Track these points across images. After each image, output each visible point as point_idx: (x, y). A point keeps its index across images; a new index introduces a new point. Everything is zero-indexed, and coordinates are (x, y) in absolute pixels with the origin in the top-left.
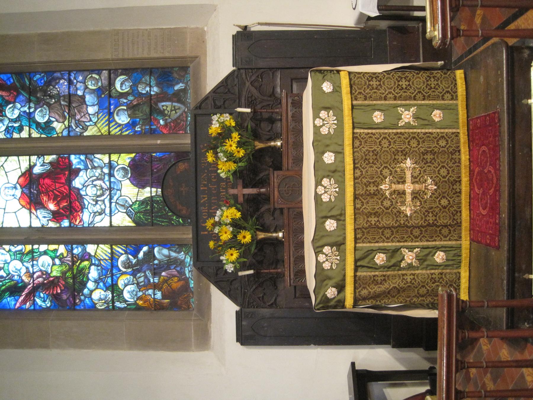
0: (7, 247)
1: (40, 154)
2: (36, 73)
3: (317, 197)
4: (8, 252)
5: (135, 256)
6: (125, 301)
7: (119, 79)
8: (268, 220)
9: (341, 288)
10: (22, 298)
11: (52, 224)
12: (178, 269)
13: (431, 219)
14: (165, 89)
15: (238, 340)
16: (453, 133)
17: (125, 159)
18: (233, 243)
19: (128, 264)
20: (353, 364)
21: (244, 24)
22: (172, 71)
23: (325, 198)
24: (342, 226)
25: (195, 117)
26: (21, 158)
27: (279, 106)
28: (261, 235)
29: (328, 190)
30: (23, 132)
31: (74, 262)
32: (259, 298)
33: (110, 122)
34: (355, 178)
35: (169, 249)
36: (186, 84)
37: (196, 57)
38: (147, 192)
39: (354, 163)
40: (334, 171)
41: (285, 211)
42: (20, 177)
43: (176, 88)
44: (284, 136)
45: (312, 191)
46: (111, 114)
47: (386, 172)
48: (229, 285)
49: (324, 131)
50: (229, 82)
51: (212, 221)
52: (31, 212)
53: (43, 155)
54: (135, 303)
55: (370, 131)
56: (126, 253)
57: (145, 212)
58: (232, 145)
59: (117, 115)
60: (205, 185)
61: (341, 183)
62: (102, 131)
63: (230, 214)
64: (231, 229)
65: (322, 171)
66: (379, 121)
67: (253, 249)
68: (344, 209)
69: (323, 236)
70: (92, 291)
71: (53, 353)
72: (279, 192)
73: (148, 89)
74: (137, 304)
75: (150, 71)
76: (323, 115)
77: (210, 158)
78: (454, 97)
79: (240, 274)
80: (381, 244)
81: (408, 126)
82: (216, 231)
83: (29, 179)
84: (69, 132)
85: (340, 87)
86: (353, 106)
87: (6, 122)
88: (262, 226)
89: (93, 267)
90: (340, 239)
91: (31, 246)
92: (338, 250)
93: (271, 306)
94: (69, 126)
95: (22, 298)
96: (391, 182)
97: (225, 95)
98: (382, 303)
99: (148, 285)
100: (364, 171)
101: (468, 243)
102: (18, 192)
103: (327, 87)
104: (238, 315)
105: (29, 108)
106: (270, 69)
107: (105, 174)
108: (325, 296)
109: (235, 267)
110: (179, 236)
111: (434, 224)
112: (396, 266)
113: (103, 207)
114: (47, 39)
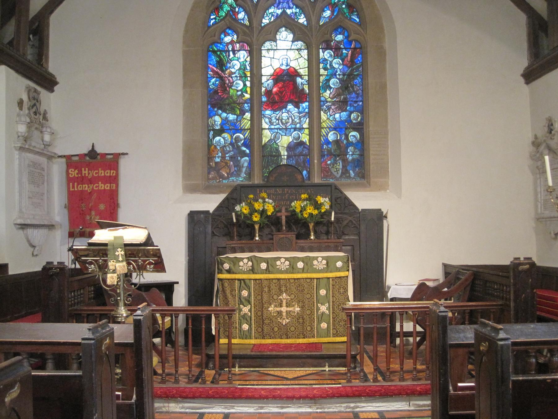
0: (248, 59)
1: (309, 82)
2: (362, 79)
3: (279, 259)
4: (245, 60)
6: (214, 138)
7: (358, 134)
8: (267, 231)
9: (229, 271)
10: (215, 69)
11: (263, 89)
12: (235, 173)
13: (266, 321)
14: (350, 164)
15: (191, 211)
16: (314, 335)
17: (305, 138)
18: (253, 211)
19: (238, 139)
20: (177, 283)
21: (388, 216)
22: (362, 170)
23: (278, 263)
24: (263, 272)
25: (330, 186)
27: (336, 238)
28: (257, 227)
29: (282, 264)
30: (323, 71)
31: (239, 104)
32: (218, 225)
33: (329, 128)
34: (289, 279)
35: (247, 167)
36: (354, 178)
37: (370, 185)
38: (284, 153)
39: (297, 279)
40: (293, 268)
41: (271, 241)
42: (294, 68)
43: (351, 172)
44: (317, 241)
45: (282, 257)
46: (335, 129)
47: (293, 296)
48: (226, 206)
49: (315, 262)
50: (352, 207)
51: (266, 196)
52: (271, 76)
53: (308, 84)
54: (212, 144)
55: (315, 288)
56: (245, 139)
57: (271, 151)
58: (310, 210)
59: (334, 133)
60: (288, 192)
61: (286, 272)
62: (324, 124)
63: (270, 210)
64: (261, 209)
65: (293, 261)
66: (321, 293)
67: (249, 222)
68: (272, 273)
69: (257, 261)
70: (220, 116)
71: (180, 92)
72: (283, 238)
73: (351, 153)
74: (211, 146)
75: (362, 155)
76: (326, 264)
77: (303, 196)
78: (335, 335)
79: (234, 214)
80: (253, 294)
81: (318, 309)
82: (260, 200)
83: (293, 74)
84: (323, 101)
85: (339, 271)
86: (329, 278)
87: (330, 59)
88: (263, 227)
89: (236, 116)
90: (256, 271)
91: (249, 75)
92: (250, 270)
93: (213, 232)
94: (327, 102)
95: (215, 69)
96: (287, 299)
97: (342, 204)
98: (220, 295)
99: (224, 153)
100: (293, 284)
101: (253, 343)
102: (284, 67)
103: (339, 264)
104: (208, 212)
105: (339, 75)
106: (359, 233)
107: (296, 125)
108: (225, 263)
109: (238, 211)
110: (256, 174)
111: (264, 325)
112: (241, 302)
113: (275, 124)
114: (383, 87)
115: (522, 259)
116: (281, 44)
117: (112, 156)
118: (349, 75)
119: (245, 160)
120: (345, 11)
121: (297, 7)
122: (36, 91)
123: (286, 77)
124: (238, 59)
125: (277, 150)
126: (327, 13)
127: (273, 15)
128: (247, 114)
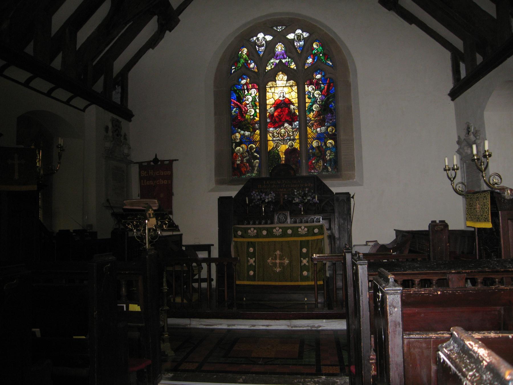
0: (258, 94)
1: (299, 108)
5: (255, 152)
6: (236, 147)
11: (268, 114)
19: (251, 148)
26: (297, 99)
38: (283, 156)
43: (329, 167)
52: (273, 104)
54: (235, 152)
56: (256, 148)
68: (270, 237)
70: (239, 133)
87: (313, 91)
94: (311, 120)
99: (243, 158)
102: (281, 99)
104: (230, 197)
105: (319, 102)
114: (349, 109)
115: (438, 222)
116: (279, 83)
117: (168, 162)
118: (325, 102)
119: (257, 162)
120: (322, 58)
121: (289, 58)
122: (118, 121)
123: (283, 105)
124: (251, 94)
125: (278, 154)
126: (310, 60)
127: (273, 64)
128: (257, 131)
